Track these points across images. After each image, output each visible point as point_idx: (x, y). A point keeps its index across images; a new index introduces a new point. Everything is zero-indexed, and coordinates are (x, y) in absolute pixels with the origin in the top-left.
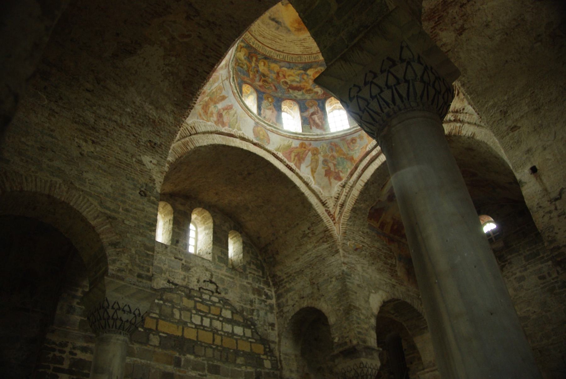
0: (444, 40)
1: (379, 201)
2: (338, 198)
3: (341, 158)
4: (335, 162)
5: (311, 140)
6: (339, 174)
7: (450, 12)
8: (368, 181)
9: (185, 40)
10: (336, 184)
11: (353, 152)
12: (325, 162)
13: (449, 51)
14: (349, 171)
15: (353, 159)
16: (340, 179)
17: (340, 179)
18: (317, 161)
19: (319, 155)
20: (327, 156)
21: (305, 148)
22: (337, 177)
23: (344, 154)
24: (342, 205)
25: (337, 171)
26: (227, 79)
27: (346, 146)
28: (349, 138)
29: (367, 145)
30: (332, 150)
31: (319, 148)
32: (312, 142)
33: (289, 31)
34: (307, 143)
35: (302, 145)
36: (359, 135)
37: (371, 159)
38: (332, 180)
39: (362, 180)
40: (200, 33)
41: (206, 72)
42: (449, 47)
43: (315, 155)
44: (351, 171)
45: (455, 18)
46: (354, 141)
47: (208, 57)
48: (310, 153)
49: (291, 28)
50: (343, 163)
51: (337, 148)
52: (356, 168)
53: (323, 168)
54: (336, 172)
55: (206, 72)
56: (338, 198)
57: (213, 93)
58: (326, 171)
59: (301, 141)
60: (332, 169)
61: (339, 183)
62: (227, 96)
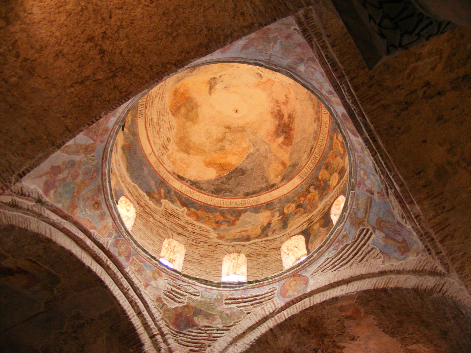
0: (282, 337)
1: (6, 257)
2: (22, 194)
3: (74, 188)
4: (68, 180)
5: (108, 142)
6: (52, 188)
7: (313, 341)
8: (55, 243)
9: (407, 71)
10: (39, 186)
11: (82, 206)
12: (72, 164)
13: (268, 343)
14: (60, 206)
15: (74, 209)
16: (46, 192)
17: (46, 192)
18: (77, 153)
19: (83, 155)
20: (79, 167)
21: (101, 134)
22: (49, 186)
23: (78, 192)
24: (14, 206)
25: (57, 184)
26: (270, 60)
27: (89, 194)
28: (101, 198)
29: (94, 228)
30: (86, 173)
31: (93, 154)
32: (104, 144)
33: (178, 81)
34: (106, 136)
35: (106, 130)
36: (105, 213)
37: (81, 240)
38: (45, 178)
39: (50, 229)
40: (402, 89)
41: (354, 78)
42: (272, 343)
43: (86, 149)
44: (61, 211)
45: (304, 345)
46: (96, 206)
47: (370, 87)
48: (91, 142)
49: (180, 83)
50: (66, 193)
51: (87, 182)
52: (65, 217)
53: (64, 162)
54: (54, 182)
55: (354, 78)
56: (22, 194)
57: (269, 43)
58: (59, 167)
59: (111, 129)
60: (61, 176)
61: (41, 192)
62: (244, 51)
